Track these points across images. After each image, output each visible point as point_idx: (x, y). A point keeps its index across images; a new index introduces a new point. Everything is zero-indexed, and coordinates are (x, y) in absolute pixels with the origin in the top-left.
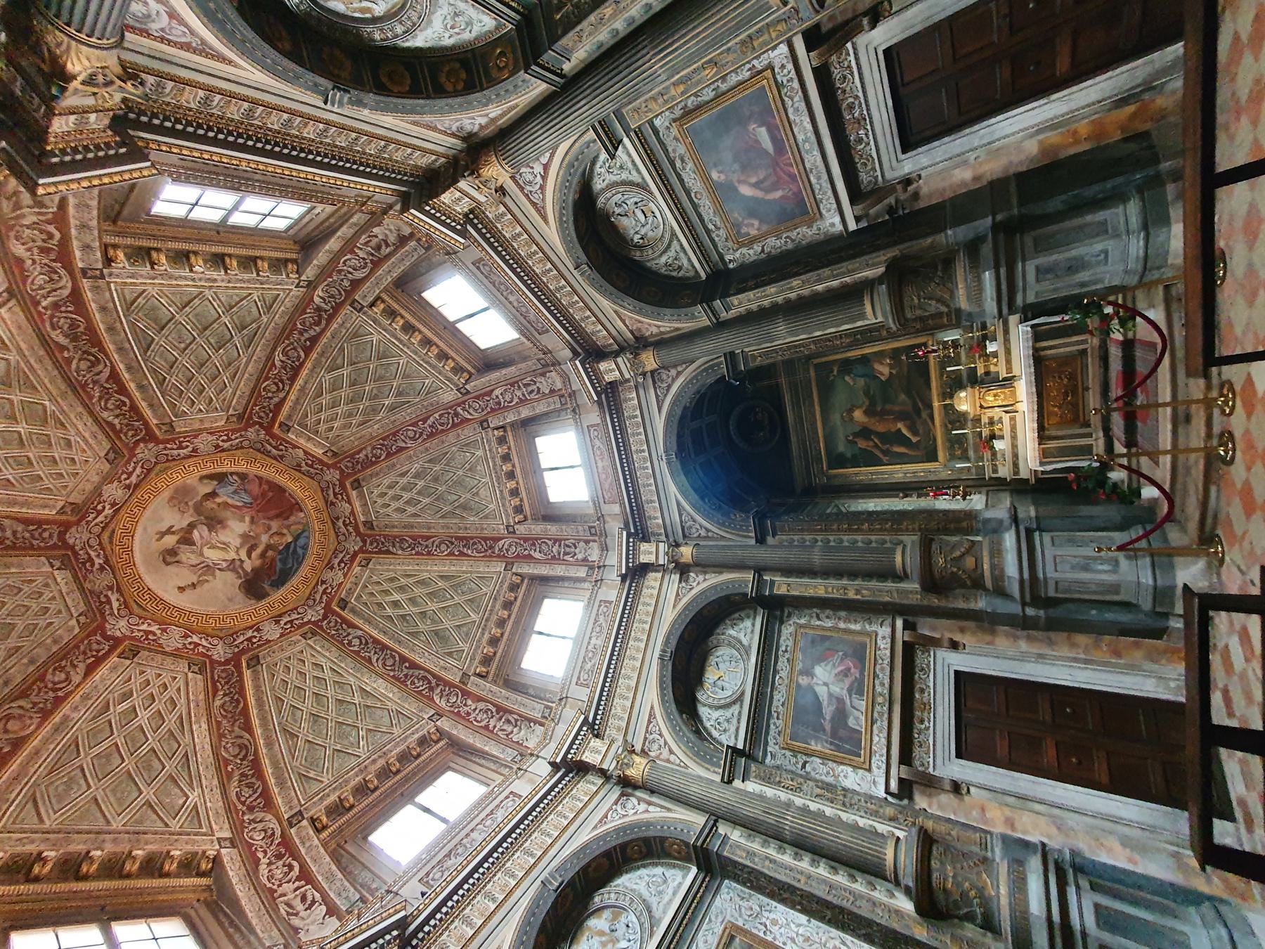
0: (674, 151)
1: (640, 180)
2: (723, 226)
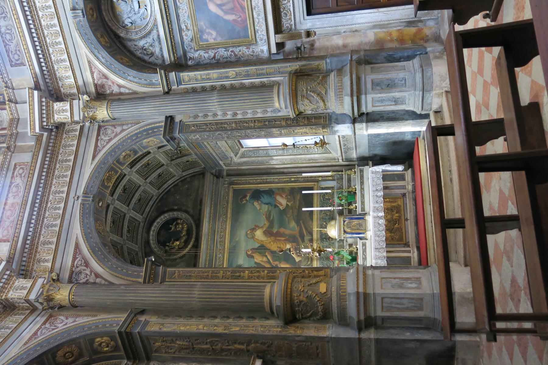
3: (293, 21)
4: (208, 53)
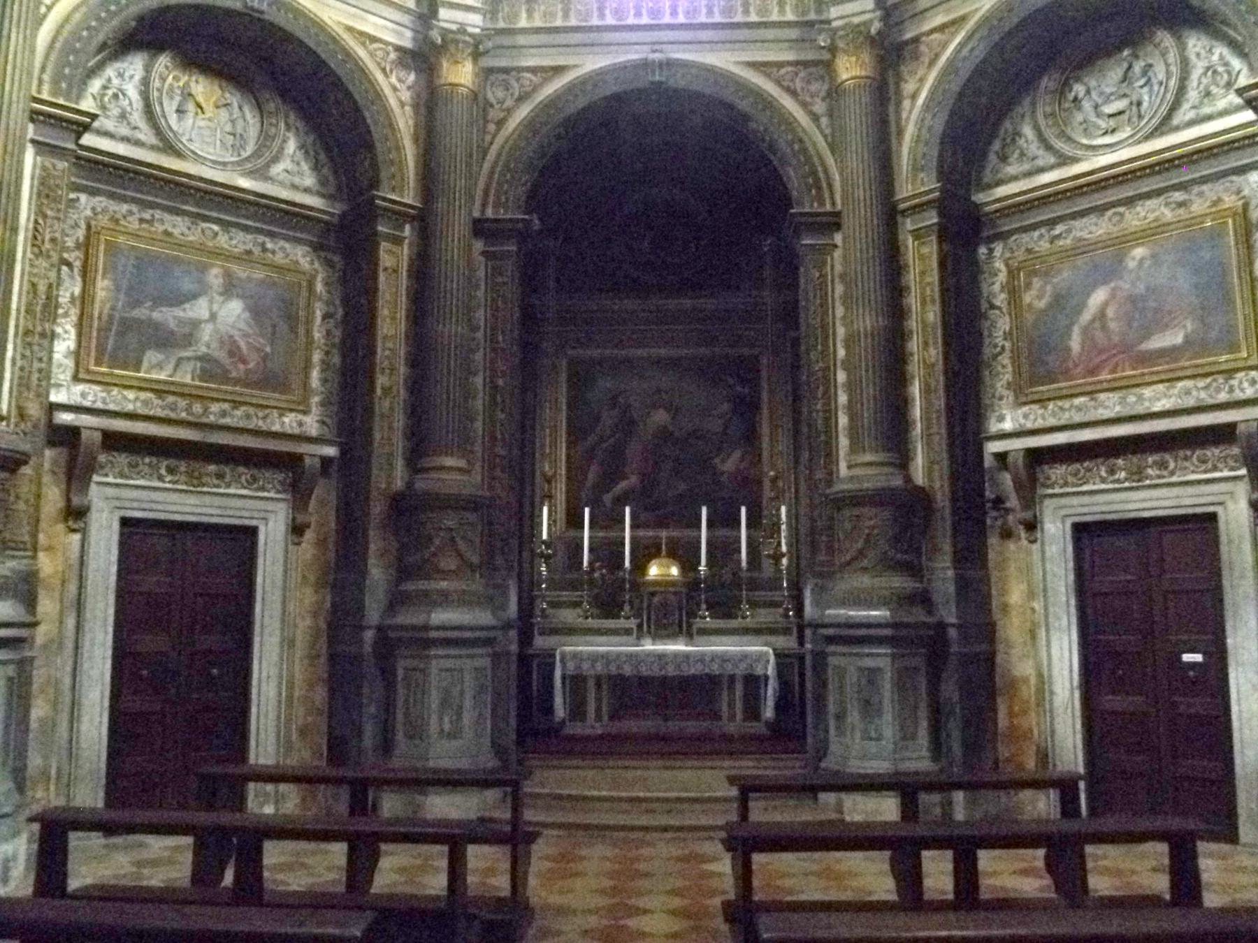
0: (1201, 194)
1: (1176, 121)
2: (1056, 249)
3: (1061, 491)
4: (1002, 291)
